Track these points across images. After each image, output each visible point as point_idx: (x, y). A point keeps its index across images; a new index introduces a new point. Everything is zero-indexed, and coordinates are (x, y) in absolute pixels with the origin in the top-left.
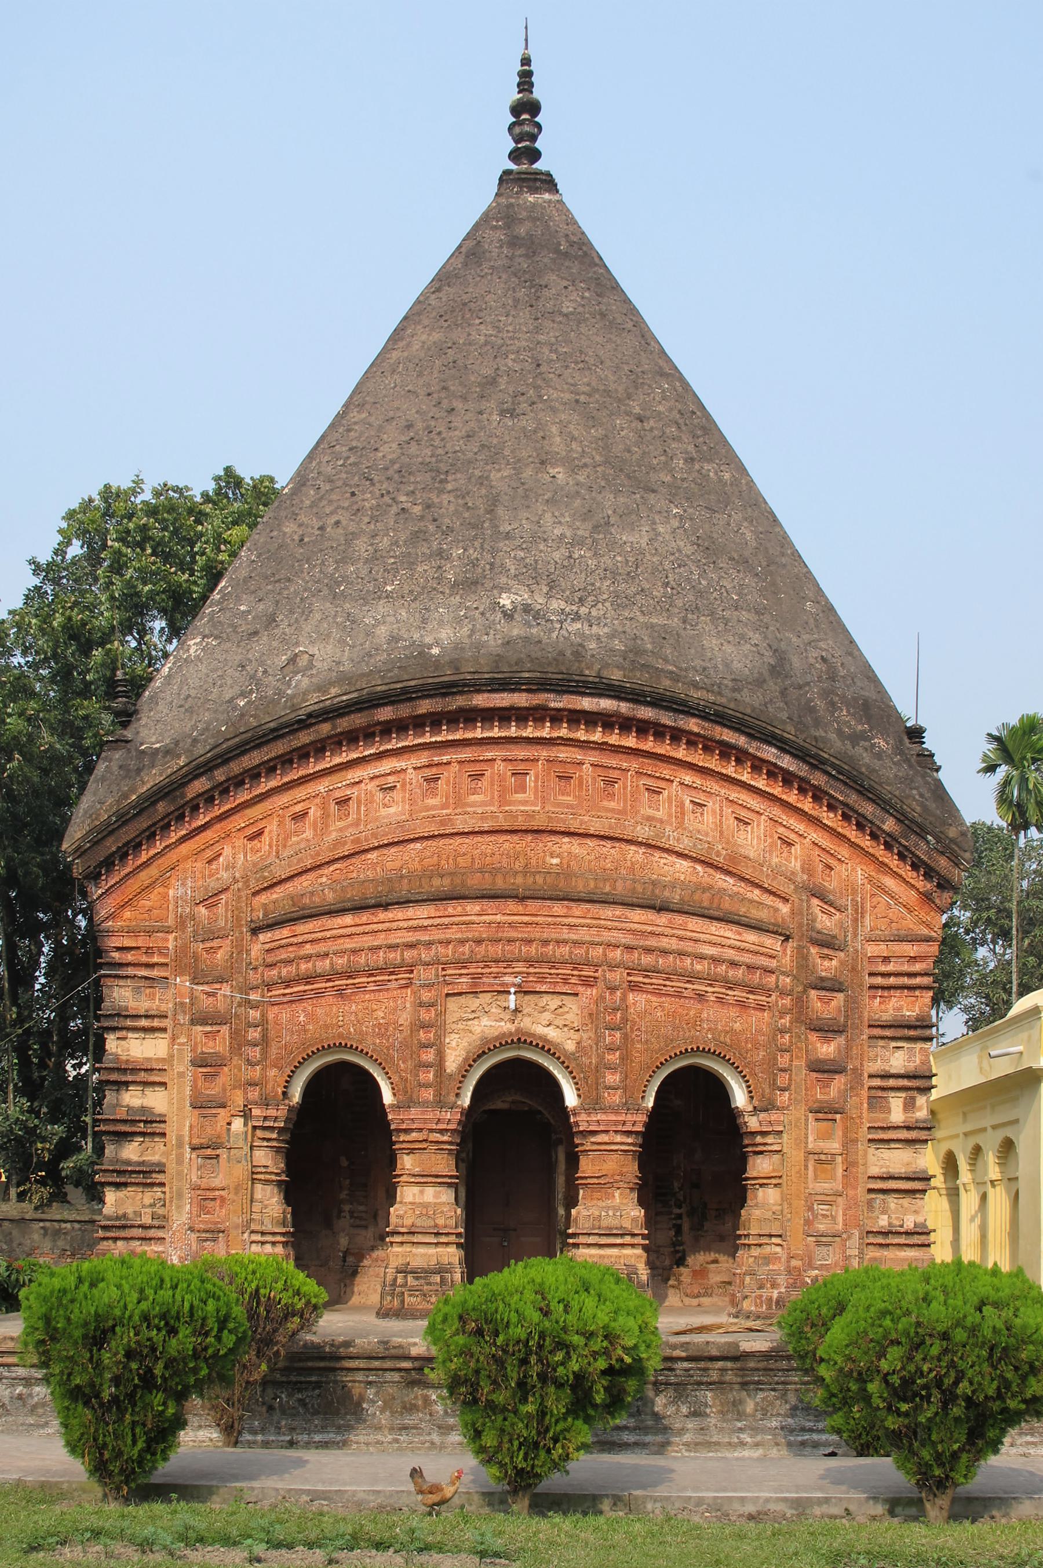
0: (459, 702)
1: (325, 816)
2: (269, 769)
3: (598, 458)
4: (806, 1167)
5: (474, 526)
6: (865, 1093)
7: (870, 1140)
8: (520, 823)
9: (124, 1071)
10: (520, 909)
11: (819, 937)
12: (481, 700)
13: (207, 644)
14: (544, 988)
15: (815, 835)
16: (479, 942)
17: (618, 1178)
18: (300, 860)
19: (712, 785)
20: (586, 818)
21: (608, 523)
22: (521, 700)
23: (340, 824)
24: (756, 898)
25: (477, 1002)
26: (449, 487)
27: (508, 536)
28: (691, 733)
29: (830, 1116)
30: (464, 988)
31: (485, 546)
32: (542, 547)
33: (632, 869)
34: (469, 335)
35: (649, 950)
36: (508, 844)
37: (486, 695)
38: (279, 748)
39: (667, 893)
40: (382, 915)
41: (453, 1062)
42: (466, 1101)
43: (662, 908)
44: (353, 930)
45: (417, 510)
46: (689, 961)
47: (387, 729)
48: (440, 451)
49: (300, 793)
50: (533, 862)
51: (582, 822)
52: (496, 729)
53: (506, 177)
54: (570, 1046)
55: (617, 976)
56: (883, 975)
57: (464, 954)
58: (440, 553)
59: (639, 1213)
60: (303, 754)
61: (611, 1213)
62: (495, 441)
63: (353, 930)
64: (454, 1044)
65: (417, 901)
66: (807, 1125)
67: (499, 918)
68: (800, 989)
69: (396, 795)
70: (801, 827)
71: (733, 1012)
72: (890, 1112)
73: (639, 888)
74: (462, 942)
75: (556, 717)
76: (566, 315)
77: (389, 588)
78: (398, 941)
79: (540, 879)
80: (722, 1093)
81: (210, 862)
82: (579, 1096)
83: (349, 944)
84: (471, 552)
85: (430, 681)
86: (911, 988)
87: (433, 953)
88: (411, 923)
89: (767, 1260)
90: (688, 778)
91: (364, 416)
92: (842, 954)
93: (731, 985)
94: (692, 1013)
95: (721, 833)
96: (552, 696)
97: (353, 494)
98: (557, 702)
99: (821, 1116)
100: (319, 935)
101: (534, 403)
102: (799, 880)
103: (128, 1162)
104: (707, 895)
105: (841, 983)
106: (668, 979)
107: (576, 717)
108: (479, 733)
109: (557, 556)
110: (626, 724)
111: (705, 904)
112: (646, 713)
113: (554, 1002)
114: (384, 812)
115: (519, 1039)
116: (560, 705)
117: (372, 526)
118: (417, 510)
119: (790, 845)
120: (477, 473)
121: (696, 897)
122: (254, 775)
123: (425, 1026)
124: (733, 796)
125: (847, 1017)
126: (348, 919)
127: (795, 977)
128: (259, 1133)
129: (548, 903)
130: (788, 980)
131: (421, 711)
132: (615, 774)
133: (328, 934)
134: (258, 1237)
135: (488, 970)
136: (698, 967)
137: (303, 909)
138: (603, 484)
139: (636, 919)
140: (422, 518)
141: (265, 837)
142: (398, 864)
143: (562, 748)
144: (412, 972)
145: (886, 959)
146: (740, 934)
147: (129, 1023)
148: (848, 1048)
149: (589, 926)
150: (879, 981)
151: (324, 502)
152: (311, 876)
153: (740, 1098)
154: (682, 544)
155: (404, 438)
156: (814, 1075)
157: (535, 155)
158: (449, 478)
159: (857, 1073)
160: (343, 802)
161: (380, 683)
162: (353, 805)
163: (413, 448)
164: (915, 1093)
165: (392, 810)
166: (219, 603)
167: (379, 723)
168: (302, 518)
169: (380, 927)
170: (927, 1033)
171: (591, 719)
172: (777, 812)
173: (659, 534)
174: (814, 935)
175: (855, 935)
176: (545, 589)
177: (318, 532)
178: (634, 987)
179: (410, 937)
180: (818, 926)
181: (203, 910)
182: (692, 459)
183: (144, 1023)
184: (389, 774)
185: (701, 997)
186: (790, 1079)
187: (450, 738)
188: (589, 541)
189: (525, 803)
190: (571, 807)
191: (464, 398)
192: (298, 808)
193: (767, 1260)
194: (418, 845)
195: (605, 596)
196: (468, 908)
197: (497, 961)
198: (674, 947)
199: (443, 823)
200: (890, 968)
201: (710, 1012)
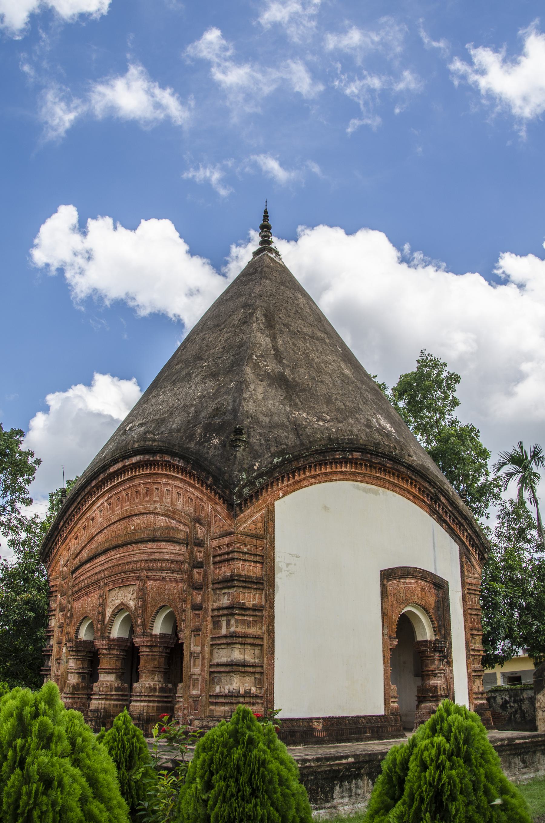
6: (209, 619)
7: (212, 645)
8: (126, 514)
12: (113, 469)
19: (170, 481)
22: (119, 465)
30: (111, 587)
49: (84, 520)
56: (220, 555)
70: (193, 490)
72: (221, 629)
81: (68, 550)
86: (228, 560)
90: (164, 480)
96: (126, 461)
106: (156, 573)
126: (88, 565)
128: (71, 653)
132: (148, 486)
134: (65, 695)
146: (175, 546)
150: (217, 559)
156: (194, 612)
159: (206, 610)
164: (230, 617)
174: (196, 541)
175: (207, 538)
180: (198, 536)
181: (65, 568)
192: (84, 525)
194: (105, 531)
201: (168, 586)
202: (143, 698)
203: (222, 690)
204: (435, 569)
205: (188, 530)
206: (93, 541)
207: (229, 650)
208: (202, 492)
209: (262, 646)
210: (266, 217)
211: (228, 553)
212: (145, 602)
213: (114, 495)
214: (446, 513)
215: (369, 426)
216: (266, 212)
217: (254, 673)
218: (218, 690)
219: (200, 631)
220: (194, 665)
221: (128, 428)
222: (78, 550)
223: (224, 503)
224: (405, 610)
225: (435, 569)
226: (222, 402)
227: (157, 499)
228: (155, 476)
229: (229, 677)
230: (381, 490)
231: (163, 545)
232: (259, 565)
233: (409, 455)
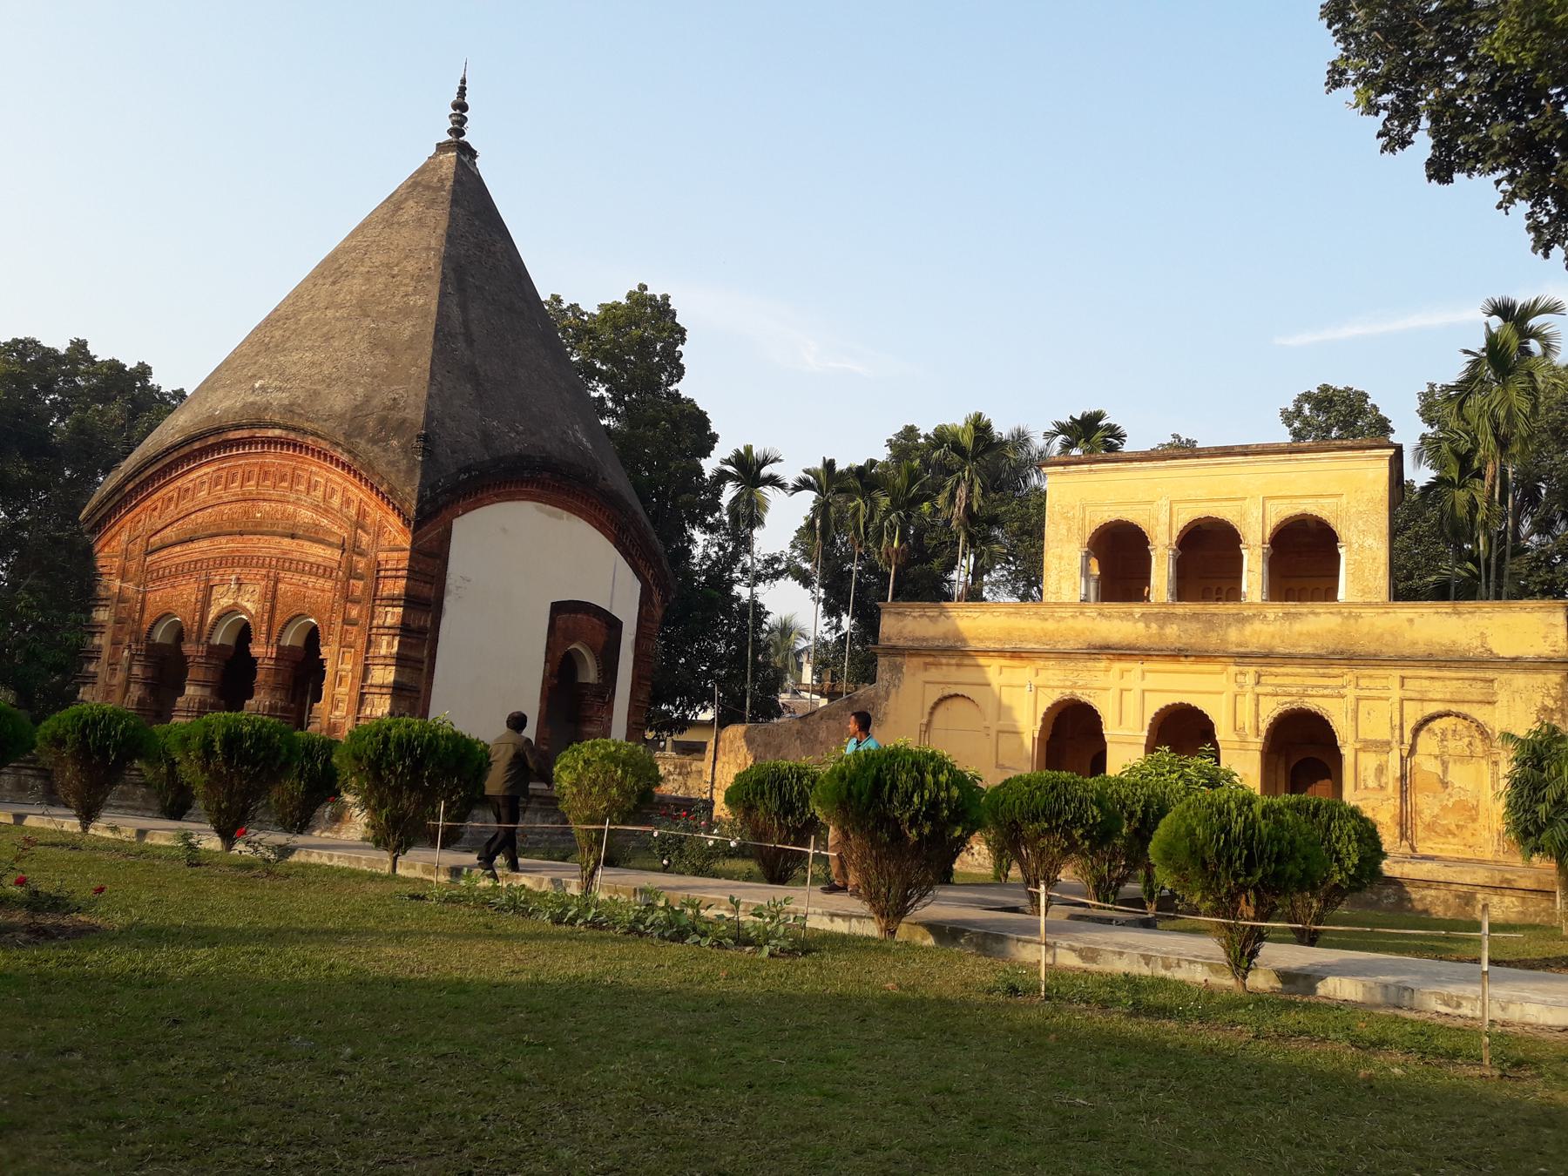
0: (224, 437)
8: (247, 496)
9: (93, 626)
12: (232, 435)
22: (245, 433)
38: (159, 466)
56: (386, 570)
96: (256, 430)
98: (259, 433)
103: (90, 672)
112: (292, 436)
126: (178, 549)
128: (136, 658)
147: (100, 603)
152: (170, 528)
183: (103, 603)
192: (170, 494)
194: (210, 510)
204: (611, 607)
205: (346, 535)
206: (186, 519)
209: (422, 670)
210: (462, 91)
212: (273, 608)
214: (634, 545)
215: (563, 441)
216: (463, 81)
217: (410, 697)
219: (352, 647)
221: (257, 385)
222: (159, 527)
223: (399, 516)
224: (572, 647)
225: (611, 607)
227: (302, 488)
230: (565, 514)
231: (307, 544)
232: (428, 586)
233: (604, 479)
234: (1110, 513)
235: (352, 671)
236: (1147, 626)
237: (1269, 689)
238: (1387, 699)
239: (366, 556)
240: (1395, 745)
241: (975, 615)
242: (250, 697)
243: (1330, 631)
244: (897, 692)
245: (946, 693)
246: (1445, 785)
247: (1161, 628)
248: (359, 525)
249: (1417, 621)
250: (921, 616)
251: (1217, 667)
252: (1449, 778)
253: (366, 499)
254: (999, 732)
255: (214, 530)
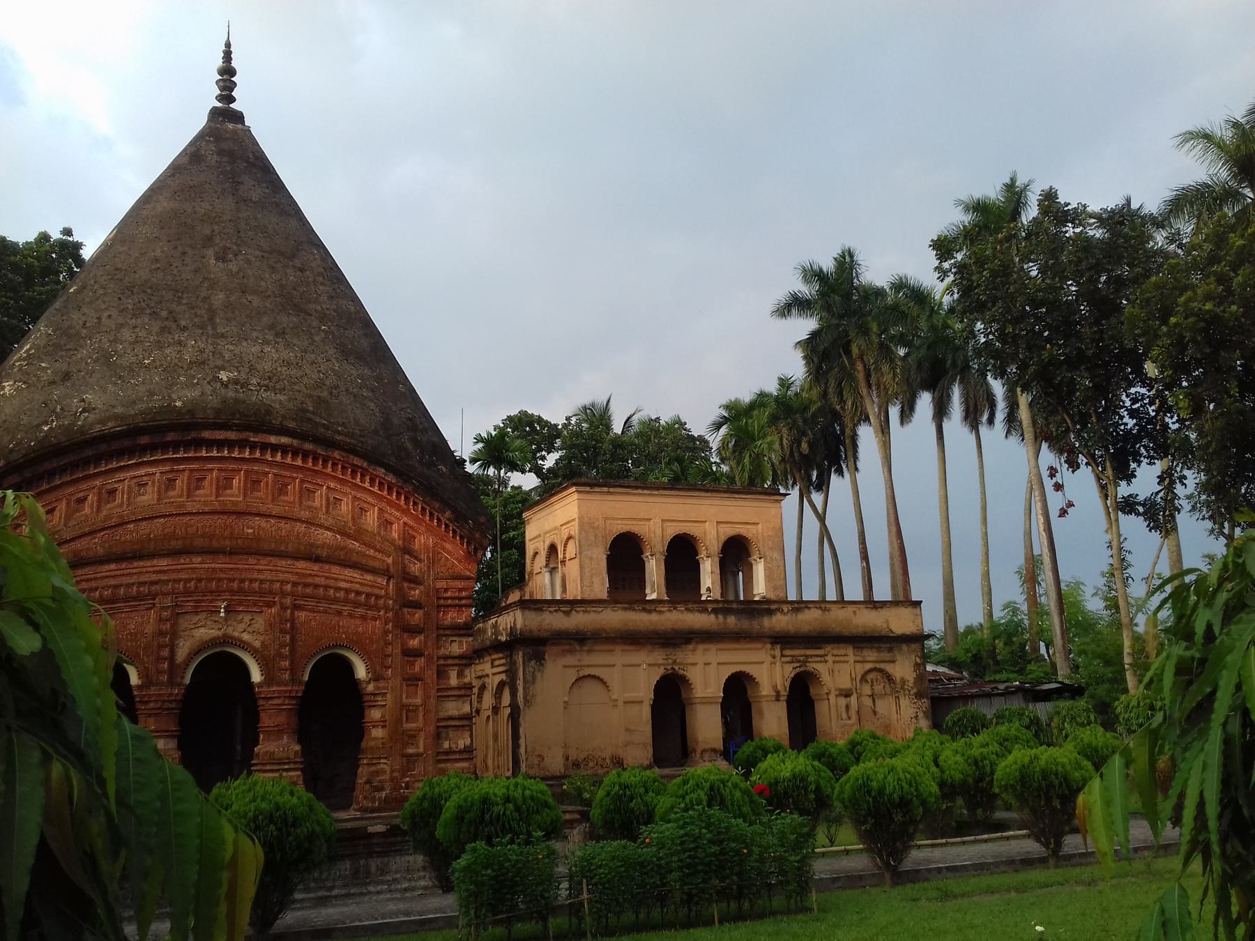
0: (194, 434)
1: (99, 500)
2: (62, 470)
3: (277, 292)
4: (401, 715)
5: (202, 328)
6: (434, 668)
8: (230, 507)
10: (228, 561)
11: (408, 577)
12: (206, 434)
13: (18, 386)
14: (241, 609)
15: (405, 519)
16: (200, 580)
17: (286, 726)
18: (80, 528)
20: (270, 506)
21: (284, 333)
22: (232, 435)
23: (109, 506)
24: (371, 554)
25: (198, 617)
26: (184, 301)
27: (223, 336)
28: (335, 458)
29: (415, 683)
31: (209, 341)
32: (244, 344)
33: (298, 535)
34: (194, 207)
35: (306, 585)
36: (220, 521)
37: (210, 432)
38: (71, 458)
39: (319, 551)
40: (136, 564)
41: (181, 655)
42: (187, 680)
43: (317, 559)
44: (116, 573)
45: (164, 314)
46: (332, 591)
47: (144, 449)
48: (178, 278)
49: (84, 487)
50: (236, 531)
51: (268, 508)
52: (215, 452)
53: (214, 113)
54: (257, 644)
55: (288, 601)
57: (190, 587)
58: (180, 343)
59: (298, 748)
60: (87, 462)
61: (281, 749)
62: (213, 276)
63: (116, 573)
64: (181, 644)
65: (160, 555)
66: (401, 690)
67: (213, 565)
68: (398, 607)
69: (149, 488)
71: (358, 622)
72: (449, 678)
73: (302, 548)
74: (190, 580)
75: (253, 447)
76: (254, 203)
77: (146, 361)
78: (146, 579)
79: (240, 542)
80: (348, 667)
82: (262, 675)
83: (112, 582)
84: (200, 343)
85: (176, 421)
86: (461, 606)
87: (170, 587)
88: (155, 568)
89: (377, 773)
90: (332, 485)
91: (125, 248)
92: (422, 587)
93: (357, 604)
94: (333, 622)
95: (352, 517)
97: (120, 299)
99: (409, 682)
100: (92, 576)
101: (236, 255)
102: (397, 543)
104: (342, 553)
105: (421, 604)
107: (264, 447)
108: (204, 454)
109: (253, 350)
110: (295, 454)
111: (342, 558)
112: (309, 446)
113: (247, 618)
114: (140, 499)
115: (224, 641)
116: (257, 440)
117: (134, 321)
118: (164, 314)
119: (391, 524)
120: (203, 294)
121: (337, 553)
122: (51, 474)
123: (161, 633)
124: (359, 495)
125: (424, 623)
126: (113, 566)
127: (395, 601)
129: (245, 557)
130: (391, 602)
131: (169, 439)
133: (98, 575)
135: (206, 598)
136: (338, 595)
137: (82, 559)
138: (280, 308)
139: (300, 566)
140: (167, 319)
141: (57, 513)
142: (147, 531)
143: (258, 464)
144: (155, 599)
145: (446, 590)
146: (362, 575)
148: (426, 642)
149: (271, 571)
150: (442, 602)
151: (100, 302)
152: (88, 538)
153: (361, 672)
154: (327, 348)
155: (153, 267)
156: (406, 658)
157: (233, 100)
158: (185, 296)
160: (112, 492)
161: (141, 420)
162: (119, 495)
163: (160, 275)
164: (462, 667)
165: (144, 498)
166: (24, 359)
167: (140, 445)
168: (84, 310)
169: (135, 571)
170: (470, 632)
171: (275, 448)
172: (384, 504)
173: (315, 341)
174: (406, 576)
175: (429, 576)
176: (247, 370)
177: (95, 321)
178: (296, 607)
179: (154, 577)
180: (407, 570)
182: (332, 297)
184: (142, 476)
185: (339, 613)
186: (392, 661)
187: (186, 455)
188: (273, 342)
189: (233, 496)
190: (261, 499)
191: (191, 247)
192: (81, 495)
193: (377, 773)
195: (284, 376)
196: (194, 559)
197: (212, 592)
198: (323, 583)
199: (178, 507)
200: (449, 594)
202: (292, 766)
203: (453, 746)
207: (460, 703)
208: (416, 518)
211: (461, 599)
213: (192, 470)
218: (446, 745)
220: (407, 719)
226: (409, 410)
228: (308, 473)
229: (459, 733)
231: (335, 569)
234: (624, 526)
235: (424, 704)
236: (717, 617)
237: (789, 659)
238: (847, 662)
239: (420, 584)
240: (854, 691)
241: (600, 609)
242: (256, 742)
243: (816, 619)
244: (542, 677)
245: (581, 674)
246: (875, 713)
247: (725, 618)
248: (406, 550)
249: (858, 612)
250: (555, 611)
251: (759, 645)
252: (877, 709)
253: (411, 523)
254: (625, 703)
255: (178, 544)
